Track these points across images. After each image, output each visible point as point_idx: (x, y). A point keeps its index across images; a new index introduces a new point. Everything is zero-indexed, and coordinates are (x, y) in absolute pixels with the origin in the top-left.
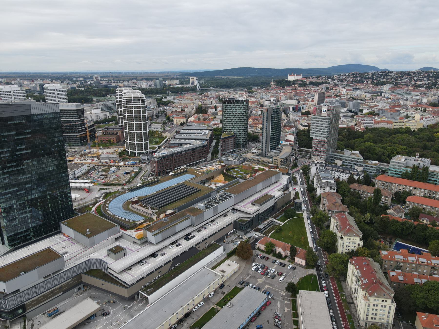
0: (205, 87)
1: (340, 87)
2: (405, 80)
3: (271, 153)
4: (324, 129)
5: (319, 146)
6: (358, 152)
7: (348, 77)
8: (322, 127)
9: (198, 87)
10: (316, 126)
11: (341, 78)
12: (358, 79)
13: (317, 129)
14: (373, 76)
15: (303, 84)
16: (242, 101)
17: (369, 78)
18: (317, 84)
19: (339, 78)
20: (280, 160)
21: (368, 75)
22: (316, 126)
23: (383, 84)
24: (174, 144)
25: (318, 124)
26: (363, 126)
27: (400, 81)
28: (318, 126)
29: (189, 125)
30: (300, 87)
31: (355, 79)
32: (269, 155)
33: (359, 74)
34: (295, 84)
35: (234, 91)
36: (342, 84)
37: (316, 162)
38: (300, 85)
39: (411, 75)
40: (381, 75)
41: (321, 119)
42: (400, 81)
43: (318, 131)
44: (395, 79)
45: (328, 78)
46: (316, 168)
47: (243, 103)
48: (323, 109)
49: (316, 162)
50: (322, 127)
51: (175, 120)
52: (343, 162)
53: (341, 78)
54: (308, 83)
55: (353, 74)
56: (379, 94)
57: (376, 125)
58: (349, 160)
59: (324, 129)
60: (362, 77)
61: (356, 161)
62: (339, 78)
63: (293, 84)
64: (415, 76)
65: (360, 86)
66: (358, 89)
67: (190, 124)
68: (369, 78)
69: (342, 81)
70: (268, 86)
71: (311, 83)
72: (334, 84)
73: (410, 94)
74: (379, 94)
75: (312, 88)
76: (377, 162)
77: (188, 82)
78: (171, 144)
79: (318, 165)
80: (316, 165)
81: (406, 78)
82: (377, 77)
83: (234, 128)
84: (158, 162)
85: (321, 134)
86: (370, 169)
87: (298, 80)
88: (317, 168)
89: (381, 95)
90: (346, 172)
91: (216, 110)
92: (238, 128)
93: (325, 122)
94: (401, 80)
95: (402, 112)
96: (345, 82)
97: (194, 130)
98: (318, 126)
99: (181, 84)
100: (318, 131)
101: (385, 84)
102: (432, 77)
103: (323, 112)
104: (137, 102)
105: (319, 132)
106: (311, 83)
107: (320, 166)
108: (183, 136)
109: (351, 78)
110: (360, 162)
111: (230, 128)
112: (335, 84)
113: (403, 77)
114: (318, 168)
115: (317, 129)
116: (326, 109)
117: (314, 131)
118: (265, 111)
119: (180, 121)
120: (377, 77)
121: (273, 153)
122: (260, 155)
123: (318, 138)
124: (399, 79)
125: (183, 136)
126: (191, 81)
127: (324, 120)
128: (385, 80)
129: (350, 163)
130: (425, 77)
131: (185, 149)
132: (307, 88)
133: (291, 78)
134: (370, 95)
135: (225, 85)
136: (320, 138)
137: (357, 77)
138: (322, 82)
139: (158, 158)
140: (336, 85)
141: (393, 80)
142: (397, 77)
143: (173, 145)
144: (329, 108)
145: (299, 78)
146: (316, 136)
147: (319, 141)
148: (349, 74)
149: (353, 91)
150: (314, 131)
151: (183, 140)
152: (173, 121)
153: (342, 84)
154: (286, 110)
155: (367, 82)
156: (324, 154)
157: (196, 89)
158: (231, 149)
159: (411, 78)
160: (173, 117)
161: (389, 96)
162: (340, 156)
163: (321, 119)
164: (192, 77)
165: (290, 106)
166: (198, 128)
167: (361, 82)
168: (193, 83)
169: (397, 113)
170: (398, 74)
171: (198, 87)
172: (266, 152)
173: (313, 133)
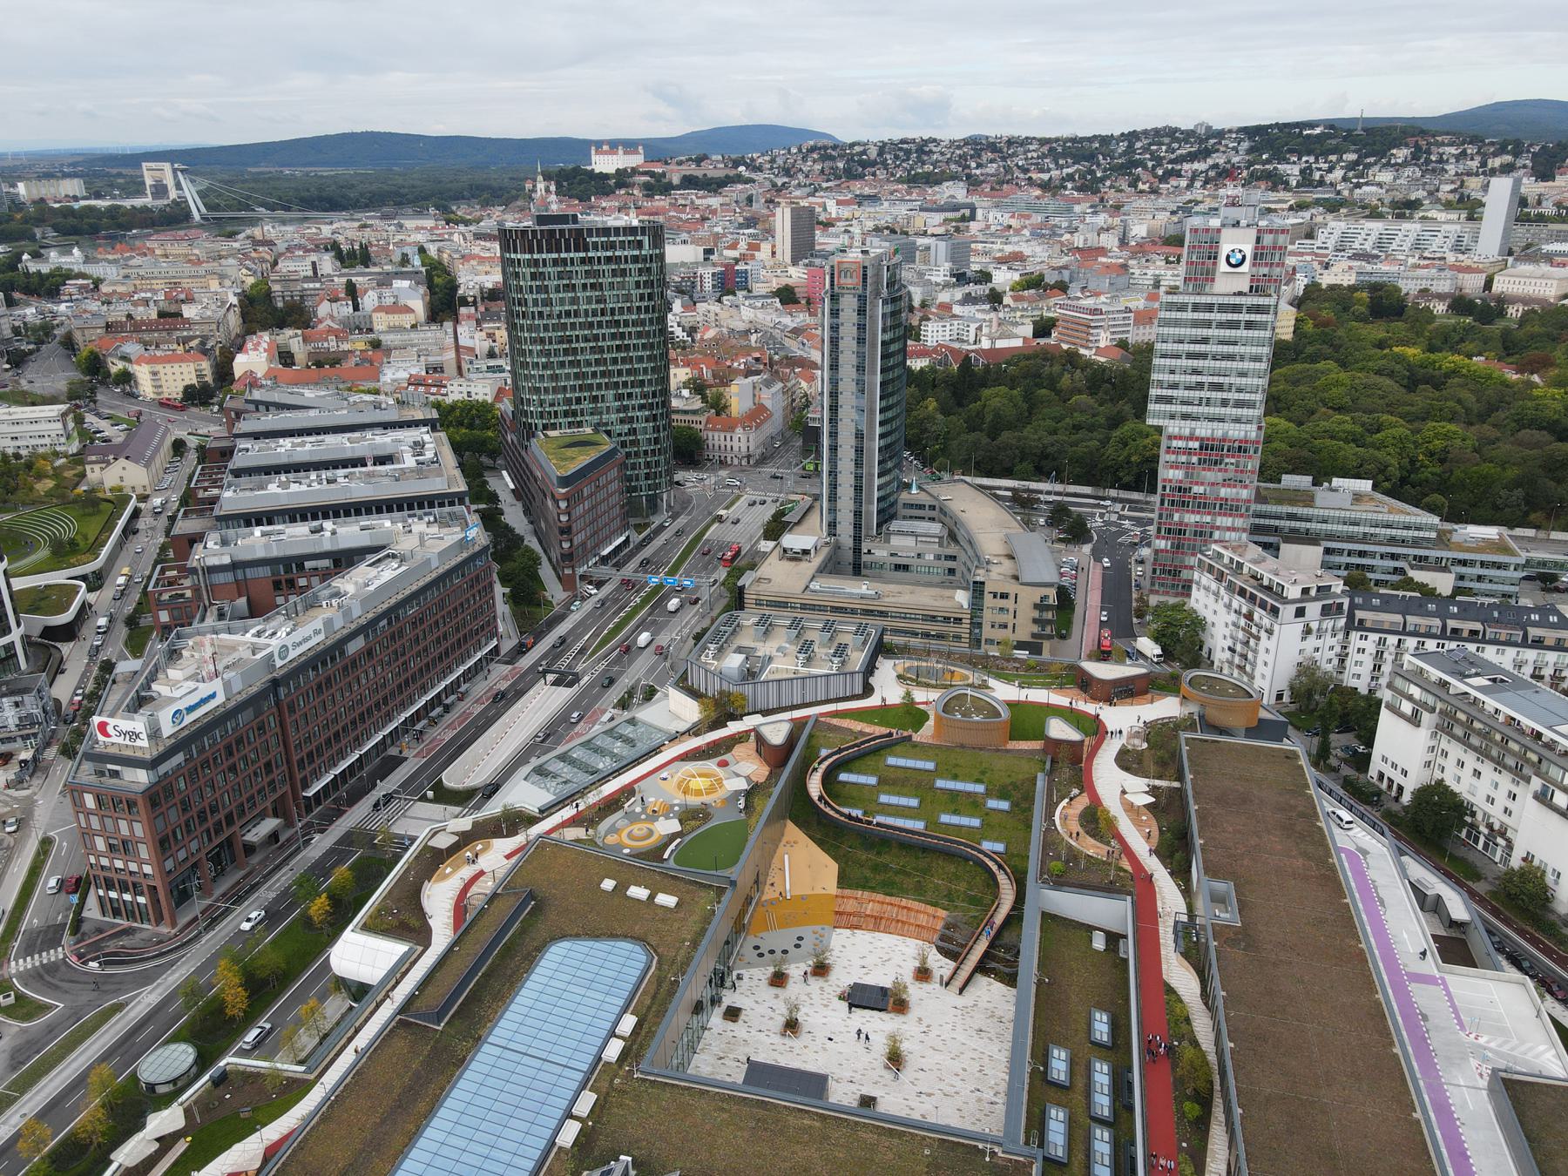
0: (230, 208)
1: (798, 193)
2: (992, 168)
3: (896, 541)
4: (1243, 374)
5: (1210, 476)
6: (1366, 485)
7: (804, 159)
8: (1230, 357)
9: (197, 209)
10: (1190, 356)
11: (780, 161)
12: (841, 165)
13: (1196, 372)
14: (881, 153)
16: (631, 230)
17: (873, 164)
18: (713, 186)
19: (773, 161)
20: (1035, 595)
21: (864, 152)
22: (1190, 356)
23: (933, 180)
24: (235, 566)
25: (1205, 341)
26: (1104, 339)
27: (978, 172)
28: (1203, 356)
29: (268, 406)
30: (650, 196)
31: (828, 164)
32: (881, 553)
33: (834, 147)
34: (632, 185)
35: (384, 217)
36: (799, 185)
37: (1293, 592)
38: (650, 190)
39: (1000, 151)
40: (908, 152)
41: (1223, 308)
42: (978, 172)
43: (1200, 386)
45: (736, 164)
46: (1298, 627)
47: (640, 245)
48: (1225, 249)
49: (1293, 592)
50: (1230, 357)
51: (142, 372)
52: (1328, 551)
53: (780, 161)
54: (676, 180)
55: (812, 149)
56: (967, 212)
57: (1141, 330)
58: (1350, 538)
59: (1243, 374)
60: (850, 160)
61: (1392, 541)
62: (773, 161)
63: (620, 185)
64: (1015, 155)
65: (858, 187)
66: (874, 199)
67: (276, 397)
68: (873, 164)
69: (787, 172)
70: (516, 198)
71: (689, 182)
72: (767, 183)
73: (1070, 210)
74: (967, 212)
75: (698, 202)
76: (1491, 532)
77: (137, 188)
78: (212, 570)
79: (1313, 609)
80: (1300, 613)
81: (992, 161)
82: (896, 157)
83: (595, 399)
84: (155, 797)
85: (1225, 403)
86: (1480, 578)
87: (635, 171)
88: (1307, 631)
89: (973, 218)
90: (1503, 634)
91: (356, 308)
92: (619, 397)
93: (1250, 325)
94: (979, 166)
95: (1137, 272)
96: (800, 176)
97: (330, 439)
98: (1203, 356)
99: (98, 196)
100: (1200, 386)
101: (938, 182)
102: (1064, 155)
103: (1223, 267)
105: (1205, 394)
106: (689, 182)
107: (1326, 611)
108: (276, 492)
110: (1416, 543)
111: (568, 401)
112: (774, 185)
113: (979, 156)
114: (1314, 626)
115: (1196, 372)
116: (1248, 250)
117: (1174, 386)
118: (848, 281)
119: (180, 376)
121: (909, 542)
122: (832, 567)
123: (1204, 430)
124: (973, 165)
125: (276, 492)
126: (149, 182)
127: (1190, 315)
128: (928, 168)
129: (1362, 554)
130: (1044, 156)
131: (360, 615)
132: (681, 202)
133: (604, 164)
134: (938, 218)
135: (321, 199)
136: (1219, 430)
137: (832, 158)
138: (727, 176)
139: (152, 765)
140: (779, 189)
141: (953, 166)
142: (963, 157)
143: (228, 577)
144: (1268, 240)
145: (636, 160)
146: (1185, 417)
147: (1207, 446)
148: (800, 150)
149: (860, 204)
150: (1174, 386)
151: (301, 530)
152: (126, 378)
153: (799, 185)
154: (686, 285)
155: (874, 174)
156: (1239, 522)
157: (187, 216)
158: (608, 539)
159: (1004, 159)
160: (124, 358)
161: (1006, 219)
162: (1292, 517)
163: (1223, 308)
164: (153, 165)
165: (700, 271)
166: (343, 416)
167: (850, 175)
168: (160, 190)
169: (1122, 280)
170: (959, 147)
171: (197, 209)
172: (857, 539)
173: (1168, 400)
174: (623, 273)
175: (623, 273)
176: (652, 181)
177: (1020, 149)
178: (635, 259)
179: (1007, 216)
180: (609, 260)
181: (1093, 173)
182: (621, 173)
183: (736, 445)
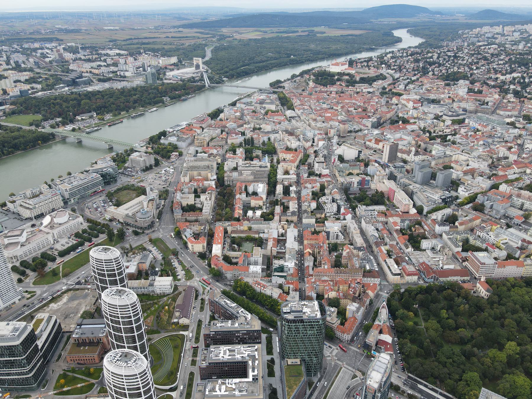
14: (438, 58)
15: (352, 82)
21: (431, 57)
30: (347, 86)
39: (488, 60)
44: (468, 66)
47: (319, 322)
54: (358, 79)
62: (396, 62)
63: (338, 80)
64: (493, 62)
68: (434, 63)
81: (483, 66)
82: (444, 59)
94: (477, 68)
104: (134, 382)
109: (411, 63)
113: (478, 63)
120: (444, 59)
124: (475, 68)
126: (195, 63)
132: (358, 90)
159: (488, 64)
164: (197, 59)
174: (313, 328)
175: (313, 328)
176: (350, 79)
177: (496, 59)
178: (317, 325)
179: (477, 124)
180: (309, 325)
181: (524, 78)
182: (339, 74)
183: (344, 338)
